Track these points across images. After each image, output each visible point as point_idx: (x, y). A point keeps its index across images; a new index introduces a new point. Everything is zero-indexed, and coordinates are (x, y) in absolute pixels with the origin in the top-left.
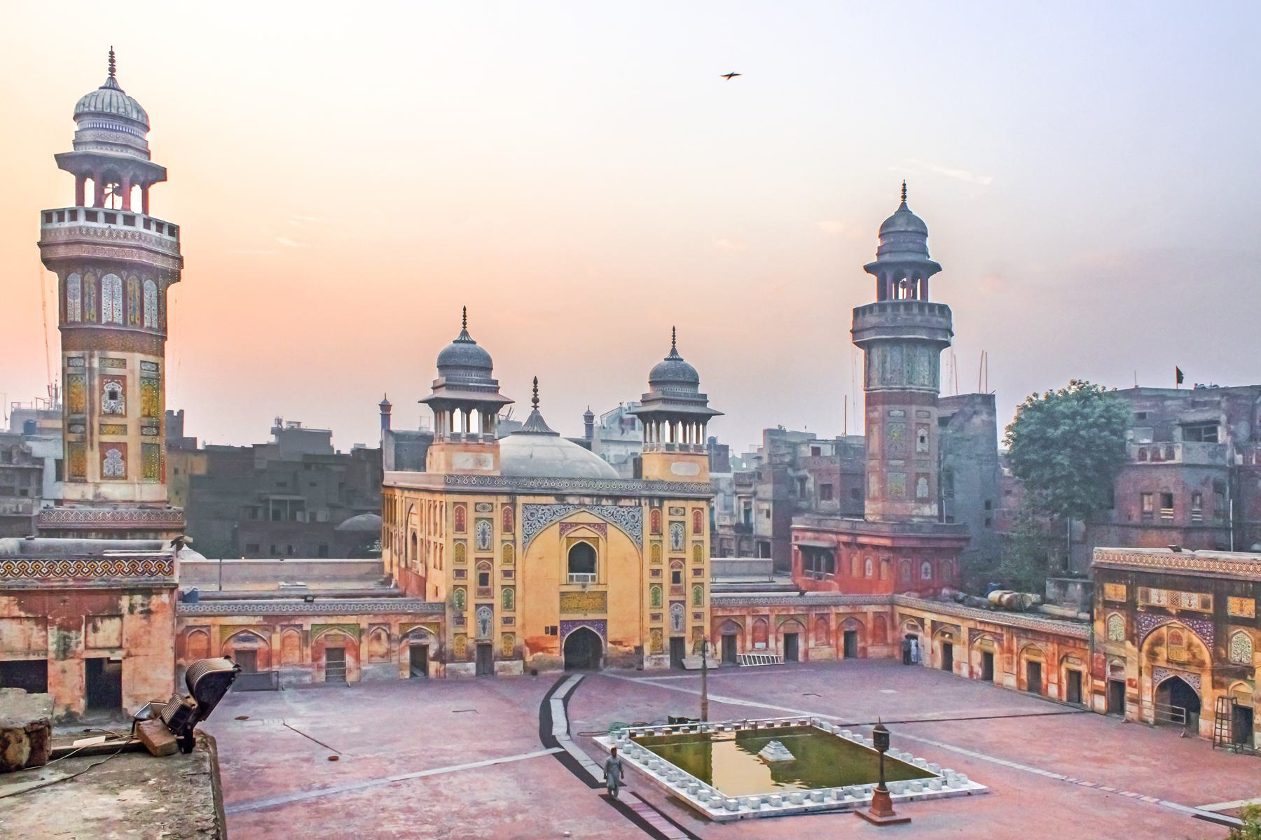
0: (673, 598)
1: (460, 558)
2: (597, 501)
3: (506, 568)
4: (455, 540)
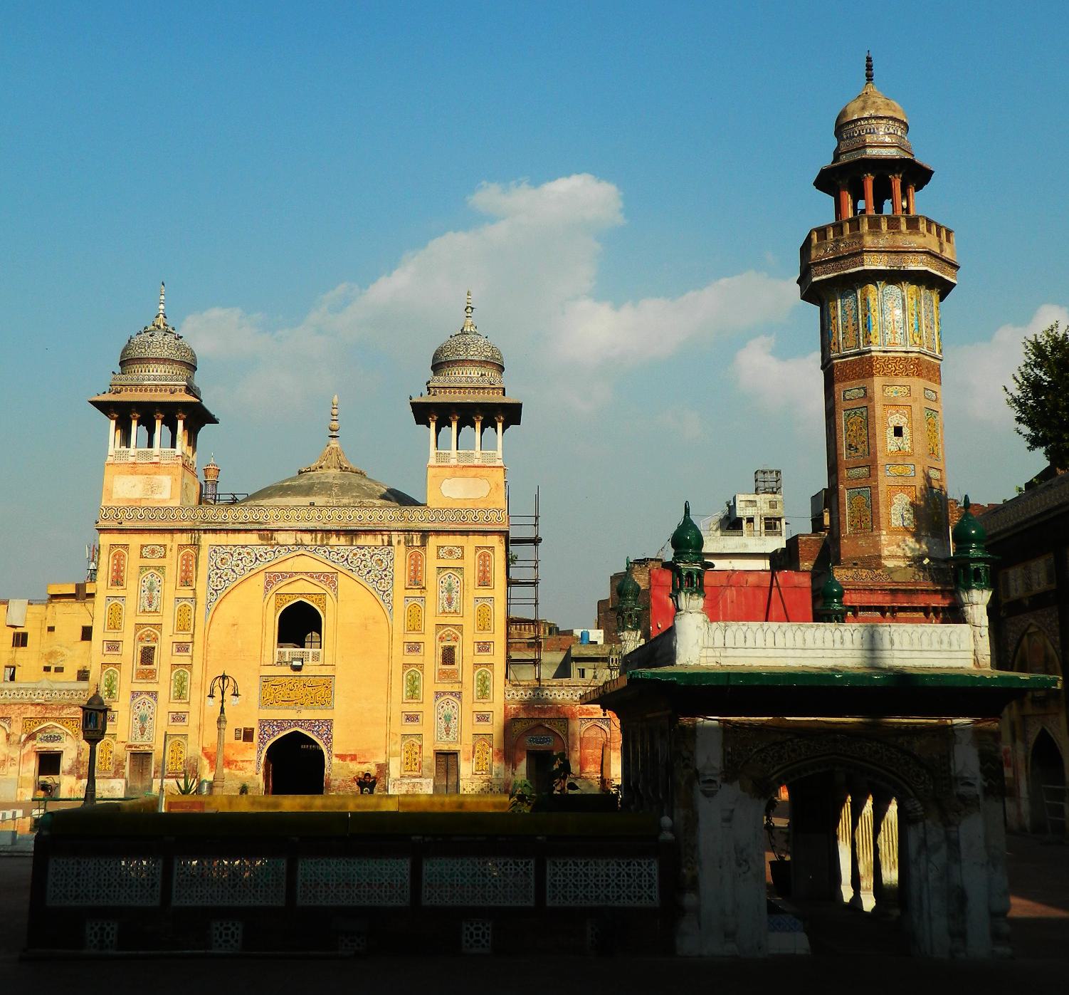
0: (441, 688)
1: (114, 625)
2: (322, 539)
3: (180, 638)
4: (109, 598)
